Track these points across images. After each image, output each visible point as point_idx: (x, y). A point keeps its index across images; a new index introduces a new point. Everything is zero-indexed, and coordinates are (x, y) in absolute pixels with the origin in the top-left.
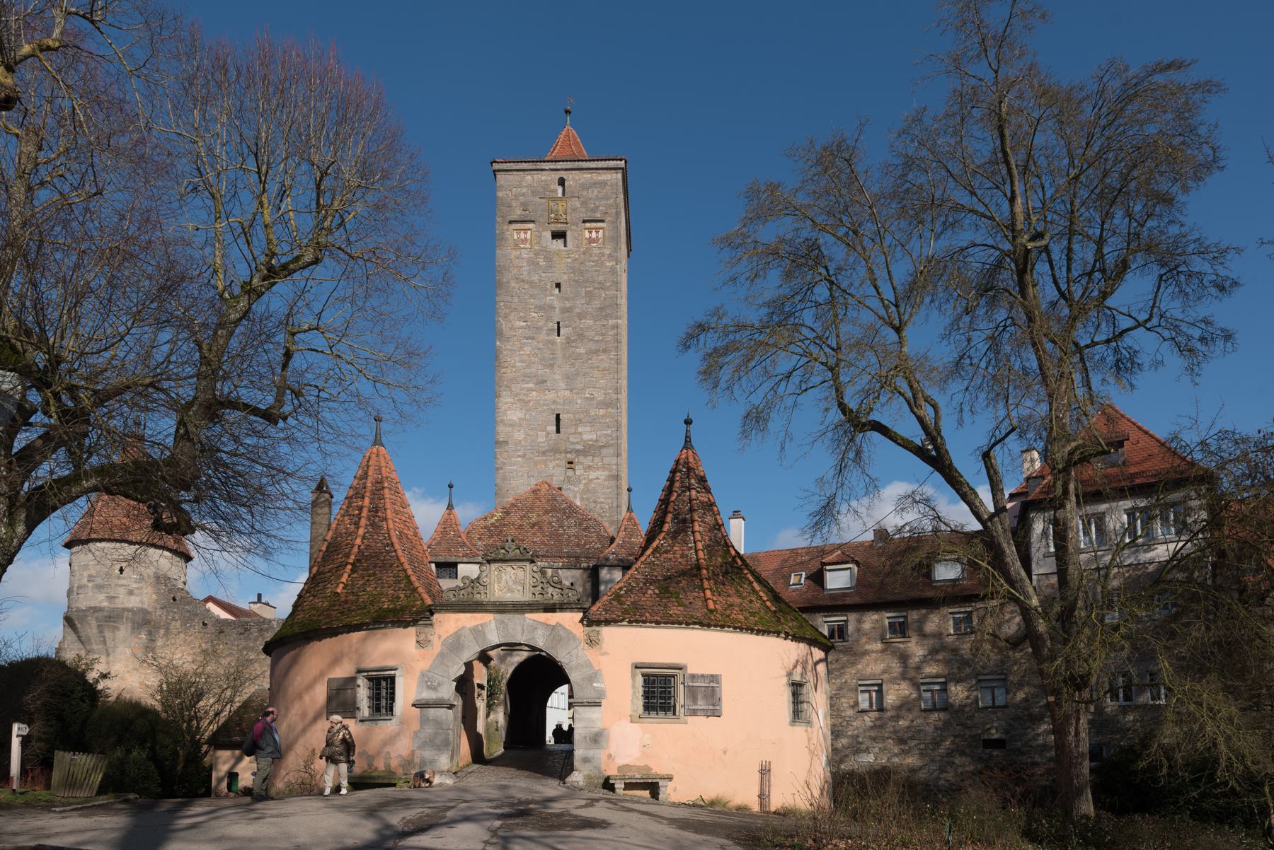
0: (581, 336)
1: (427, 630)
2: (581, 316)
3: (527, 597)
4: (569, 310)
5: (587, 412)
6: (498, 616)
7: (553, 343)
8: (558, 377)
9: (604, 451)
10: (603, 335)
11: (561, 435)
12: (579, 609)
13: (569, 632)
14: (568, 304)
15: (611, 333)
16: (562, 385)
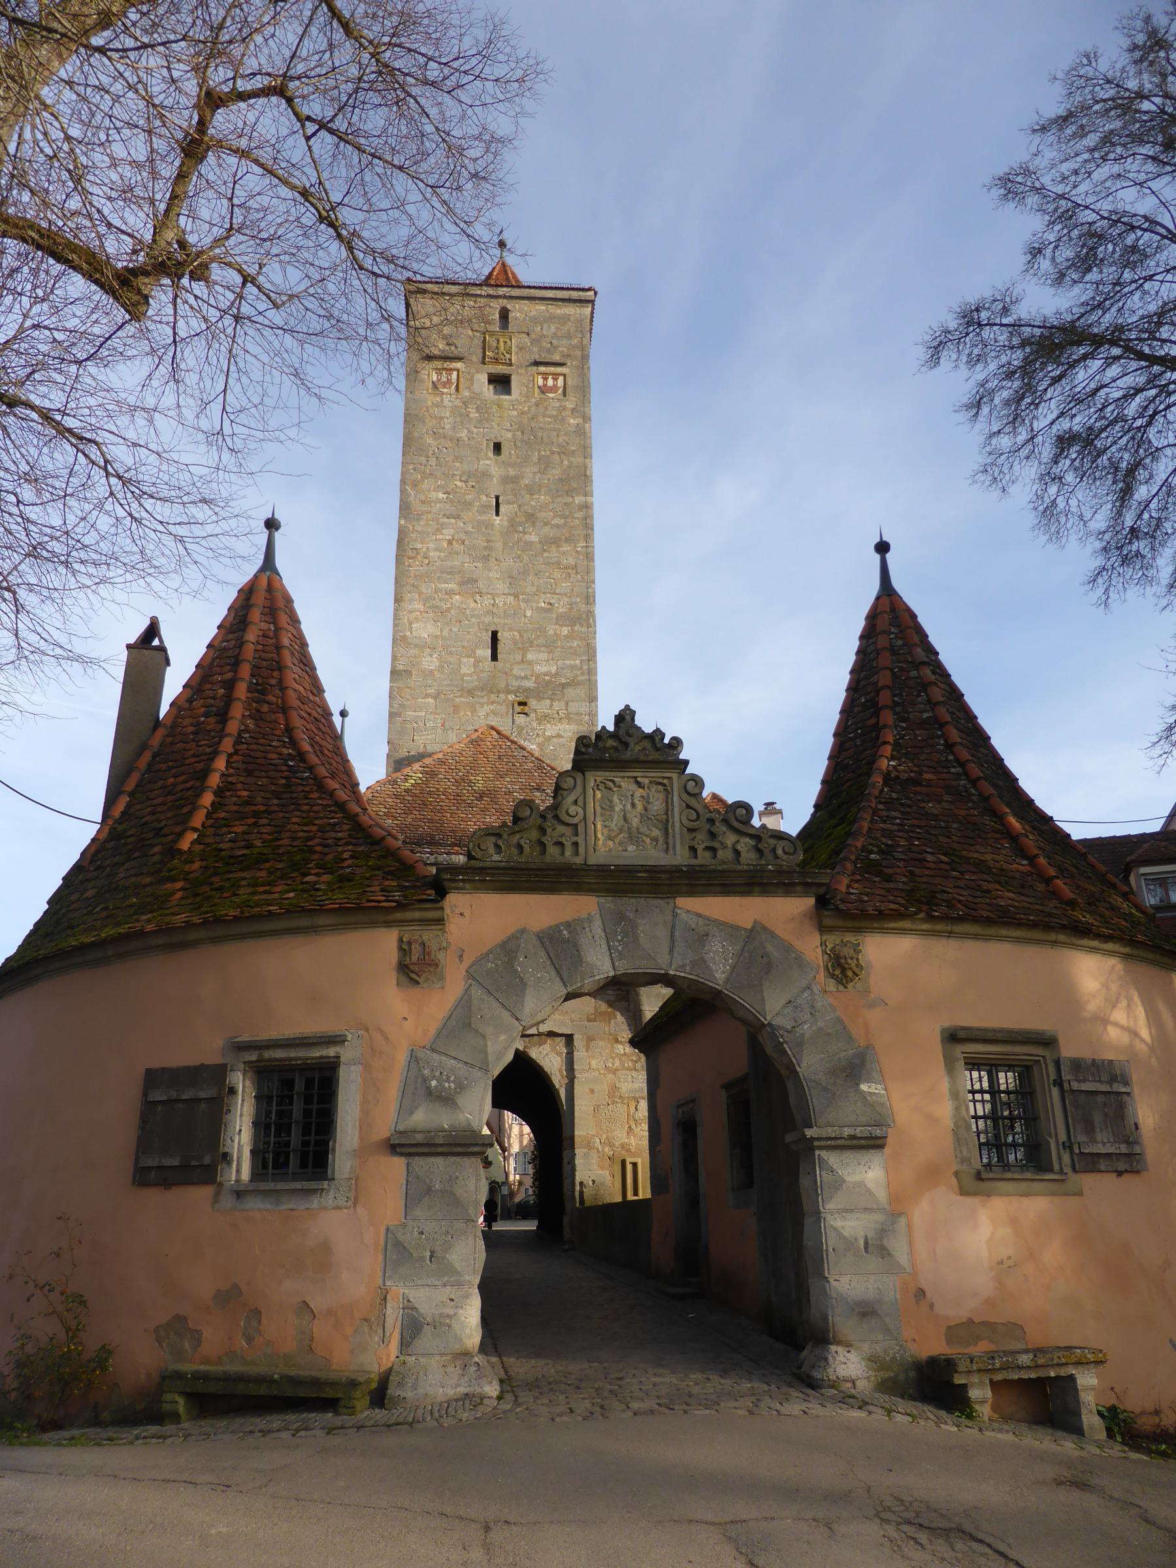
0: (531, 518)
1: (428, 935)
2: (531, 490)
3: (680, 857)
4: (514, 480)
5: (542, 630)
6: (608, 902)
7: (489, 525)
8: (493, 574)
9: (571, 692)
10: (564, 517)
11: (499, 664)
12: (807, 888)
13: (788, 949)
14: (512, 472)
15: (579, 515)
16: (501, 587)
